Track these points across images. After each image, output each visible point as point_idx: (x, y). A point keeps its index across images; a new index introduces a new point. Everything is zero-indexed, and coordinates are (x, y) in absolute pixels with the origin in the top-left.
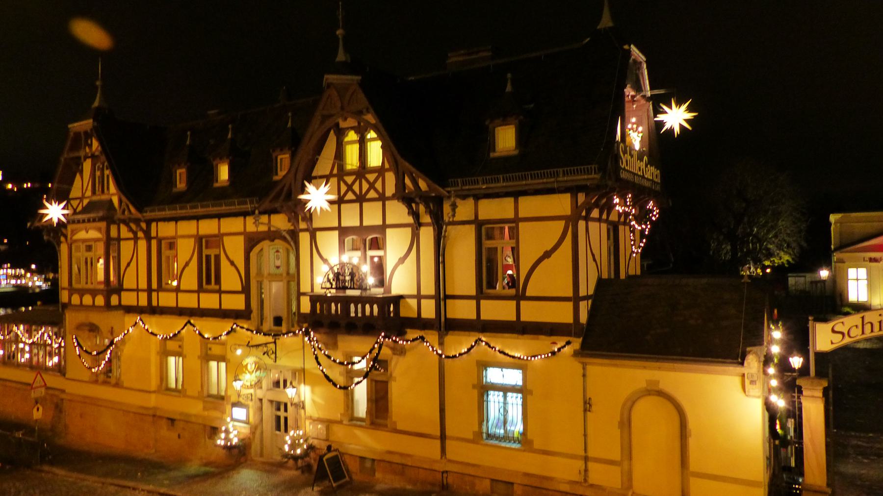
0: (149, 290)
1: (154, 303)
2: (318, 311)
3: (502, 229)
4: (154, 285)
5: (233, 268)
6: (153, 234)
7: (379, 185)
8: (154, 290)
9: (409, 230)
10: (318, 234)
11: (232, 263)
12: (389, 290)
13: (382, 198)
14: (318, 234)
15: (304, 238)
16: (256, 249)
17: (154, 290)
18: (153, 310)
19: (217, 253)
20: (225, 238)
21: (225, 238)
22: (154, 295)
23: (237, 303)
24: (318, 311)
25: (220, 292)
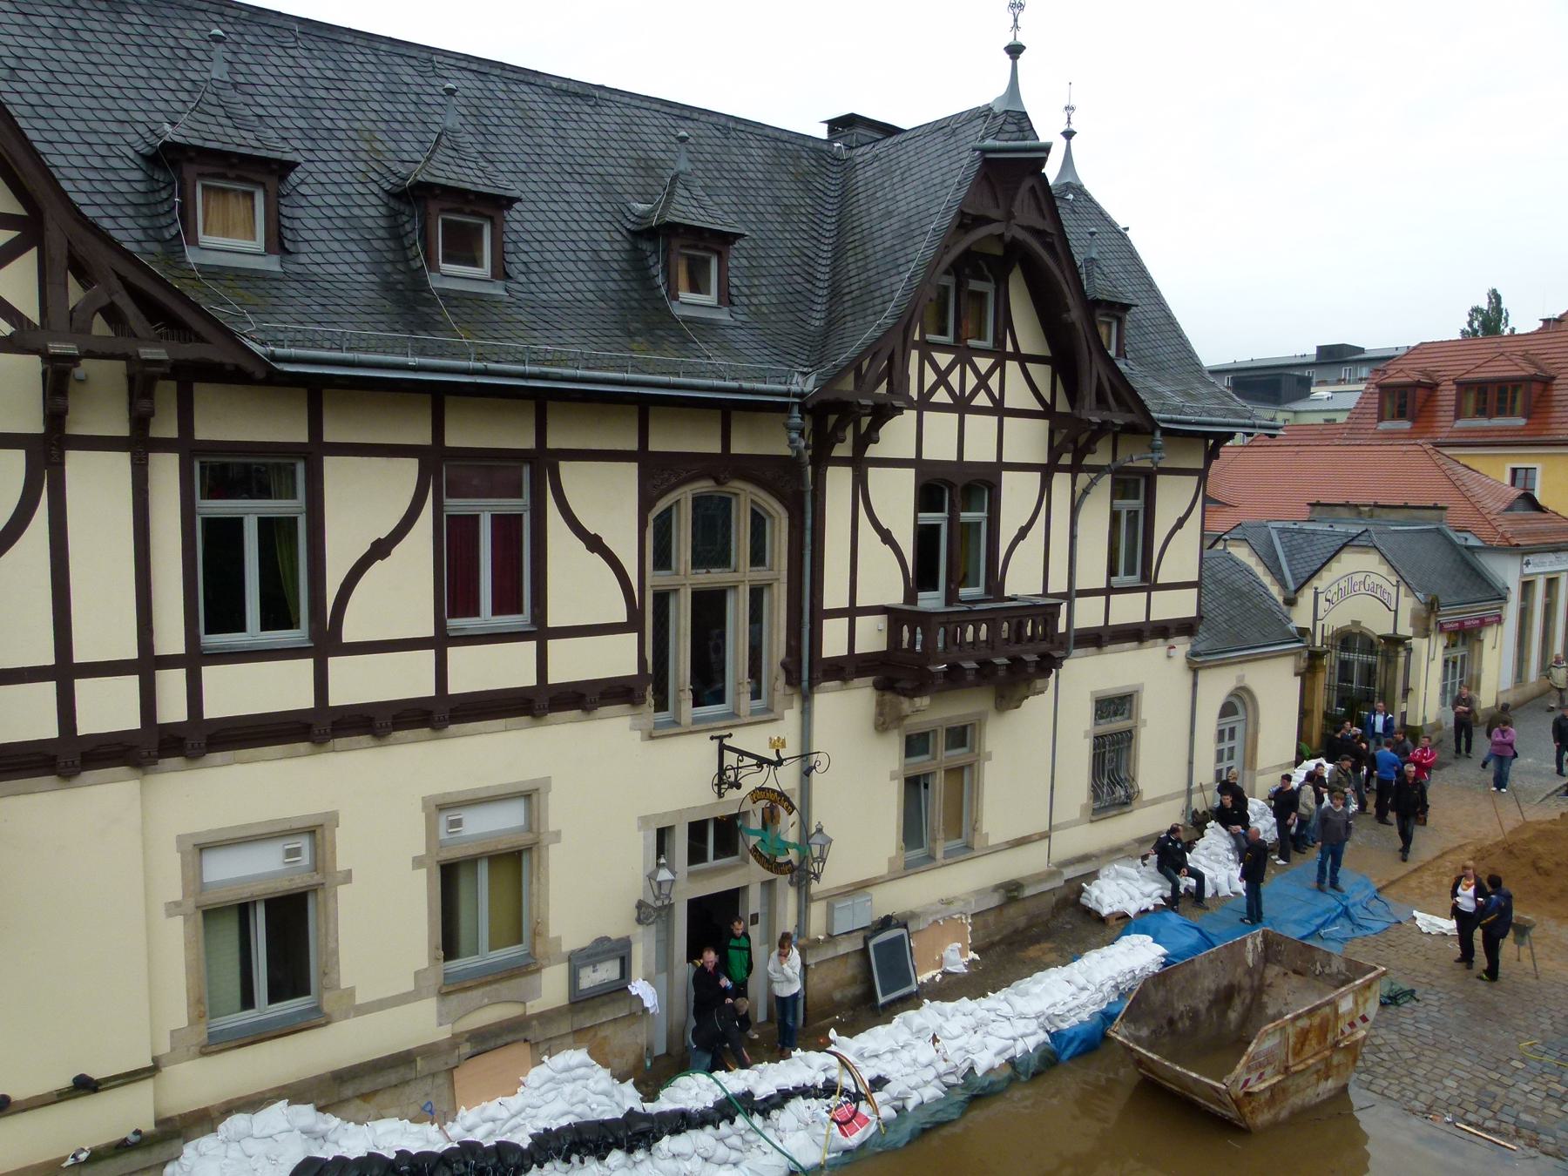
0: (146, 665)
1: (172, 709)
2: (905, 645)
3: (1137, 482)
4: (171, 638)
5: (597, 558)
6: (165, 427)
7: (994, 383)
8: (170, 662)
9: (1037, 475)
10: (872, 471)
11: (594, 544)
12: (995, 585)
13: (999, 410)
14: (872, 471)
15: (838, 482)
16: (661, 506)
17: (170, 662)
18: (150, 747)
19: (519, 505)
20: (567, 470)
21: (567, 470)
22: (172, 684)
23: (618, 657)
24: (905, 645)
25: (541, 633)
